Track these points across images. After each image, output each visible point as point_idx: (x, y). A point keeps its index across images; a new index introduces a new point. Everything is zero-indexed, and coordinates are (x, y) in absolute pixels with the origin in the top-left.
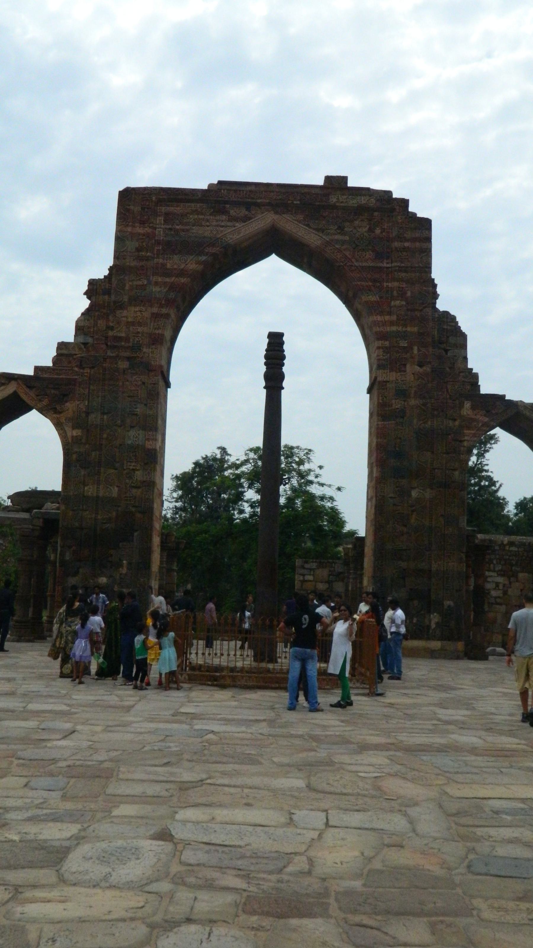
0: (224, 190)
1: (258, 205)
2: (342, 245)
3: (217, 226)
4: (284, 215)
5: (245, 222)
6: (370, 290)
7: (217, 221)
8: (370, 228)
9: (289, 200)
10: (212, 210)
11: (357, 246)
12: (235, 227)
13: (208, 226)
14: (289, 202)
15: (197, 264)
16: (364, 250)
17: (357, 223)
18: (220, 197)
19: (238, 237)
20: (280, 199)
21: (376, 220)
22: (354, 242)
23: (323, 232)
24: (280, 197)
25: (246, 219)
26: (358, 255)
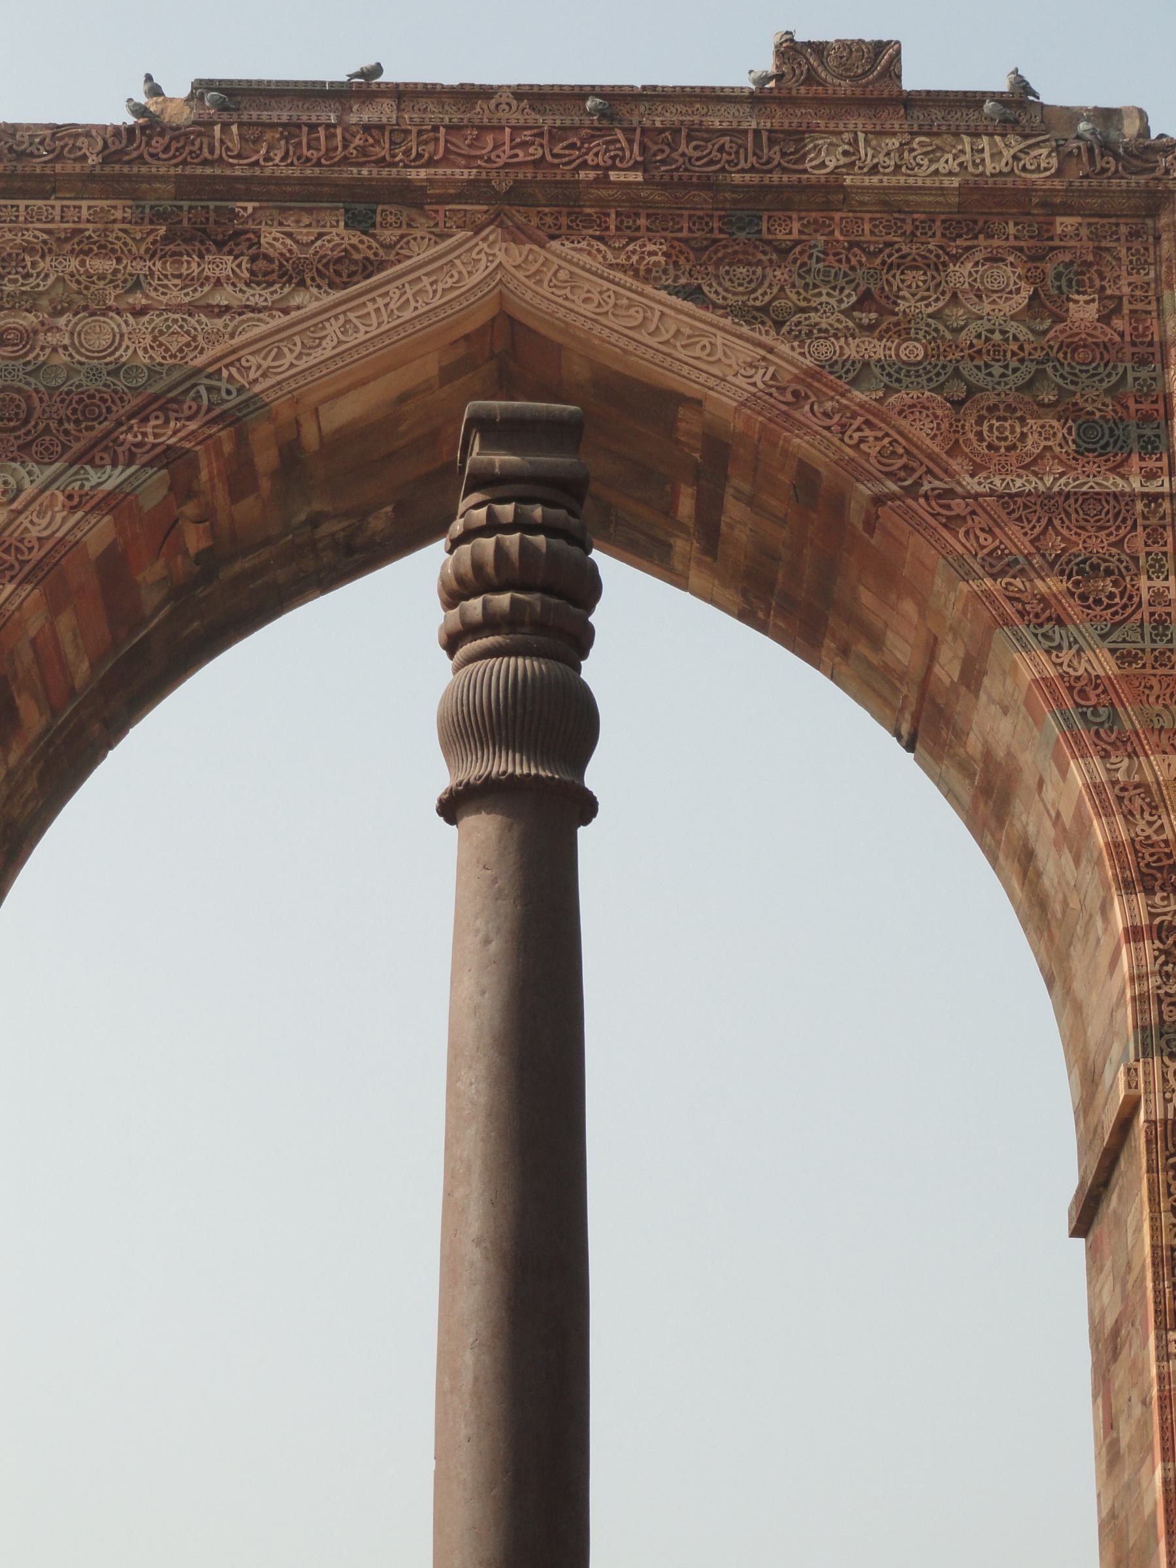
0: (226, 126)
1: (412, 197)
2: (889, 390)
3: (192, 309)
4: (555, 245)
5: (345, 285)
6: (1060, 622)
7: (188, 281)
8: (1034, 297)
9: (584, 165)
10: (162, 230)
11: (972, 390)
12: (286, 311)
13: (139, 312)
14: (582, 175)
15: (73, 509)
16: (1010, 408)
17: (961, 274)
18: (205, 162)
19: (302, 364)
20: (539, 163)
21: (1067, 258)
22: (957, 373)
23: (778, 325)
24: (535, 152)
25: (342, 271)
26: (980, 435)
